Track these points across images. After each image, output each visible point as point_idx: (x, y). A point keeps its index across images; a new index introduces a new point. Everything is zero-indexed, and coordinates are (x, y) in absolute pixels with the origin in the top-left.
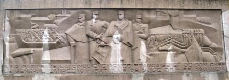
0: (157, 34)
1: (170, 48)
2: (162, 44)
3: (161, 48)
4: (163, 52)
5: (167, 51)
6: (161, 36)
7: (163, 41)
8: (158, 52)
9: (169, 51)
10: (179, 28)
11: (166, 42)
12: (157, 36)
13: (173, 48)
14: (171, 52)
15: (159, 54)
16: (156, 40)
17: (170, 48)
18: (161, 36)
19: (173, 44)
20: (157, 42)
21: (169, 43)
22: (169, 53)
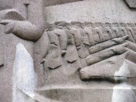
0: (73, 23)
1: (121, 72)
2: (91, 58)
3: (87, 71)
4: (95, 86)
5: (111, 80)
6: (87, 29)
7: (94, 48)
8: (79, 86)
9: (119, 82)
11: (106, 52)
12: (74, 29)
13: (132, 71)
14: (125, 87)
15: (82, 91)
16: (69, 44)
17: (121, 72)
18: (87, 29)
19: (127, 57)
20: (73, 48)
21: (116, 54)
22: (116, 88)
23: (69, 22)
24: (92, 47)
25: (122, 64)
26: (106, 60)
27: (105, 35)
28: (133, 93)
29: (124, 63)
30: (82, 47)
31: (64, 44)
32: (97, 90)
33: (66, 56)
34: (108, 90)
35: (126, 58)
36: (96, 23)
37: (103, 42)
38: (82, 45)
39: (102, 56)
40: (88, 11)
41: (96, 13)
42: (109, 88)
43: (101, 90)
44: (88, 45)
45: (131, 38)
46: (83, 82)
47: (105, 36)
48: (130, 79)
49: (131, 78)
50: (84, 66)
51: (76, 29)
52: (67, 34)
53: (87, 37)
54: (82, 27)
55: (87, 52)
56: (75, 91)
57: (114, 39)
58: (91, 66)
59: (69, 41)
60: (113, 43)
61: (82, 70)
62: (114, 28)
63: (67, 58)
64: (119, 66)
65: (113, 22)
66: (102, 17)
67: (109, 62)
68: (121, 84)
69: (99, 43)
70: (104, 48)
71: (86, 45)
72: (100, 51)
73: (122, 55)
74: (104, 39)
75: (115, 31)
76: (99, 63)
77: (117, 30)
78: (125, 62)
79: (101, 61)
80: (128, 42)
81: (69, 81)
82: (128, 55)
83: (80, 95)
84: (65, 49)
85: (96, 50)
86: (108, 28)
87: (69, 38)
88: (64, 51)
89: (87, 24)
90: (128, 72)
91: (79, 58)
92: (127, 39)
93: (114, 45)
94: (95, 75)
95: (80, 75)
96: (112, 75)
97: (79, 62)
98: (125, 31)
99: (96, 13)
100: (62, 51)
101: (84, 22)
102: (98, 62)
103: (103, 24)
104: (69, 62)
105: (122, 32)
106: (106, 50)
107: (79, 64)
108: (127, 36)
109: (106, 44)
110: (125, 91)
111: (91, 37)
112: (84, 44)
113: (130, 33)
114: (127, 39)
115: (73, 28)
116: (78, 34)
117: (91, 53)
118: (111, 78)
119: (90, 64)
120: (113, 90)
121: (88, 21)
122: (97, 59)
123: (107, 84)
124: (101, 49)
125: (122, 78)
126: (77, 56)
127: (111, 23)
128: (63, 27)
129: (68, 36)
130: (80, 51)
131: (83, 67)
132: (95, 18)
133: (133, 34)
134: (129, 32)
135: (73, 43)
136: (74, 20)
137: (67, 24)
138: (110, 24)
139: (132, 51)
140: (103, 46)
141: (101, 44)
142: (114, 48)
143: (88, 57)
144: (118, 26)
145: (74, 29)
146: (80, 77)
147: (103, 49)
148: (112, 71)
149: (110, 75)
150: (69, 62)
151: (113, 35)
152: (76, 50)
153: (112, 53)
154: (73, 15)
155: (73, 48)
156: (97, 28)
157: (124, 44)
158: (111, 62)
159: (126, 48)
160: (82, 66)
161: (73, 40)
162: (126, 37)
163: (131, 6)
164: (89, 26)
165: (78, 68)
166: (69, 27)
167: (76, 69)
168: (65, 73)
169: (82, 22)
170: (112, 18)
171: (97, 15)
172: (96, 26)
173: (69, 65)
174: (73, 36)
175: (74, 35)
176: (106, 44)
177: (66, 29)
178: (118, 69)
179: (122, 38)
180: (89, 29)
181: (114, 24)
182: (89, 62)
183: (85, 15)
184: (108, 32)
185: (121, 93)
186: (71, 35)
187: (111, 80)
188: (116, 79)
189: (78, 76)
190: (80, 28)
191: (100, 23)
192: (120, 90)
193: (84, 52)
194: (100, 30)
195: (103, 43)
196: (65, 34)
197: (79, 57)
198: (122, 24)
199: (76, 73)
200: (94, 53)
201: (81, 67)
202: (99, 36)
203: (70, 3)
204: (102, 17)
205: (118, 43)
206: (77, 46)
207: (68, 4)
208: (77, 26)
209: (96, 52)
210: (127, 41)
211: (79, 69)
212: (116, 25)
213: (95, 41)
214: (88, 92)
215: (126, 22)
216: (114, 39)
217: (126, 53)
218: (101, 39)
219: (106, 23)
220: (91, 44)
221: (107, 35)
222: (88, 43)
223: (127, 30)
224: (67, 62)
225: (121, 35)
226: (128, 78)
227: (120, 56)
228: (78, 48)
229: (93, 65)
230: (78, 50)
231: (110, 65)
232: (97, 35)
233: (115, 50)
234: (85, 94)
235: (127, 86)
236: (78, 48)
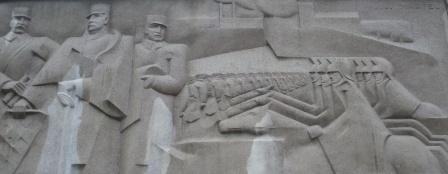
0: (214, 75)
2: (232, 110)
3: (227, 124)
4: (234, 139)
5: (252, 133)
6: (229, 80)
7: (235, 99)
9: (261, 134)
10: (296, 54)
12: (214, 80)
13: (275, 122)
14: (268, 139)
15: (218, 144)
16: (209, 96)
17: (262, 123)
18: (229, 80)
20: (213, 100)
21: (259, 104)
23: (210, 73)
31: (203, 97)
32: (235, 143)
45: (276, 88)
50: (224, 119)
56: (213, 144)
61: (221, 123)
62: (258, 78)
63: (206, 111)
64: (261, 117)
70: (246, 99)
71: (227, 97)
80: (272, 92)
86: (251, 78)
89: (229, 75)
90: (272, 124)
92: (272, 88)
104: (207, 115)
107: (218, 116)
109: (248, 95)
110: (266, 143)
114: (272, 88)
119: (230, 117)
120: (252, 143)
142: (257, 99)
146: (219, 130)
153: (254, 103)
157: (268, 94)
167: (213, 123)
170: (257, 67)
173: (208, 118)
176: (248, 95)
178: (259, 120)
188: (257, 130)
192: (260, 142)
193: (225, 103)
198: (267, 74)
205: (261, 93)
211: (218, 122)
221: (250, 85)
230: (218, 102)
231: (251, 117)
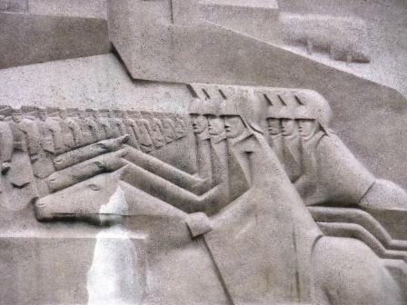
0: (25, 110)
1: (112, 205)
2: (57, 178)
3: (49, 204)
4: (62, 233)
5: (92, 222)
6: (51, 121)
7: (62, 159)
8: (34, 233)
9: (108, 224)
10: (163, 75)
12: (26, 120)
13: (132, 204)
14: (119, 234)
15: (38, 242)
16: (17, 150)
17: (112, 205)
18: (51, 121)
19: (128, 176)
20: (23, 159)
21: (105, 170)
22: (102, 235)
23: (18, 107)
24: (59, 158)
25: (114, 190)
26: (82, 183)
27: (84, 133)
28: (132, 245)
29: (119, 188)
30: (40, 157)
31: (7, 151)
33: (9, 173)
34: (87, 240)
35: (122, 180)
36: (69, 110)
37: (78, 148)
38: (41, 152)
39: (78, 174)
40: (54, 84)
41: (70, 90)
42: (89, 236)
43: (74, 240)
44: (52, 153)
45: (133, 139)
46: (40, 224)
47: (84, 136)
48: (128, 219)
49: (129, 216)
50: (44, 194)
51: (30, 121)
52: (13, 131)
53: (50, 137)
54: (41, 118)
55: (50, 167)
56: (26, 241)
57: (102, 142)
58: (56, 194)
59: (17, 145)
60: (100, 149)
61: (40, 202)
62: (103, 120)
63: (11, 178)
64: (110, 194)
65: (100, 108)
66: (80, 98)
67: (90, 186)
68: (111, 228)
69: (73, 149)
70: (82, 159)
71: (49, 153)
72: (74, 164)
73: (116, 172)
74: (83, 141)
75: (104, 126)
76: (71, 188)
77: (108, 125)
78: (119, 187)
79: (76, 185)
80: (127, 148)
81: (14, 223)
82: (126, 172)
83: (35, 250)
84: (9, 161)
85: (66, 162)
86: (90, 120)
87: (17, 139)
88: (5, 165)
89: (51, 111)
90: (125, 206)
91: (34, 179)
92: (126, 141)
93: (101, 153)
94: (63, 212)
95: (36, 210)
96: (95, 212)
97: (34, 186)
98: (123, 126)
99: (70, 90)
100: (4, 164)
101: (44, 108)
102: (71, 185)
103: (82, 111)
104: (15, 186)
105: (117, 128)
106: (86, 162)
107: (35, 189)
108: (126, 135)
110: (118, 243)
111: (59, 137)
112: (46, 151)
113: (132, 131)
114: (126, 141)
115: (25, 120)
116: (35, 133)
117: (57, 169)
118: (93, 217)
119: (54, 191)
120: (95, 240)
121: (52, 107)
122: (69, 180)
123: (85, 228)
124: (76, 160)
125: (113, 217)
126: (32, 174)
127: (96, 109)
128: (6, 116)
129: (14, 136)
130: (37, 164)
131: (42, 196)
132: (68, 98)
133: (137, 132)
134: (130, 128)
135: (25, 148)
136: (27, 103)
137: (13, 111)
138: (95, 111)
139: (134, 165)
140: (80, 154)
141: (76, 152)
142: (100, 159)
143: (52, 177)
144: (109, 116)
145: (26, 120)
146: (36, 214)
147: (80, 162)
148: (95, 205)
149: (91, 211)
150: (15, 186)
151: (100, 134)
152: (29, 164)
153: (97, 169)
154: (25, 92)
155: (23, 159)
156: (69, 119)
157: (120, 152)
158: (95, 186)
159: (124, 160)
160: (40, 193)
161: (23, 142)
162: (123, 137)
163: (135, 77)
164: (54, 116)
165: (31, 197)
166: (17, 117)
167: (28, 200)
168: (8, 207)
169: (41, 107)
170: (99, 100)
171: (71, 94)
172: (70, 116)
173: (15, 192)
174: (24, 136)
175: (25, 133)
177: (12, 121)
178: (106, 201)
179: (116, 140)
180: (55, 122)
181: (101, 111)
182: (53, 186)
183: (48, 92)
184: (90, 127)
185: (110, 245)
186: (21, 133)
187: (92, 222)
188: (102, 218)
189: (31, 214)
190: (38, 120)
191: (76, 110)
192: (109, 240)
193: (45, 166)
194: (76, 124)
195: (80, 149)
196: (9, 130)
197: (35, 176)
198: (116, 112)
199: (28, 207)
200: (63, 169)
201: (38, 195)
202: (74, 135)
203: (19, 68)
204: (80, 98)
205: (108, 150)
206: (31, 155)
207: (14, 68)
208: (33, 115)
209: (67, 167)
210: (125, 145)
211: (34, 201)
212: (106, 114)
213: (66, 145)
214: (51, 244)
215: (125, 109)
216: (102, 142)
217: (122, 169)
218: (77, 141)
219: (88, 110)
220: (58, 151)
221: (88, 133)
222: (52, 150)
223: (126, 125)
224: (11, 187)
225: (114, 133)
226: (124, 217)
227: (112, 174)
228: (33, 158)
229: (60, 192)
230: (33, 162)
231: (92, 193)
232: (70, 135)
233: (103, 164)
234: (44, 247)
235: (122, 232)
236: (33, 158)
